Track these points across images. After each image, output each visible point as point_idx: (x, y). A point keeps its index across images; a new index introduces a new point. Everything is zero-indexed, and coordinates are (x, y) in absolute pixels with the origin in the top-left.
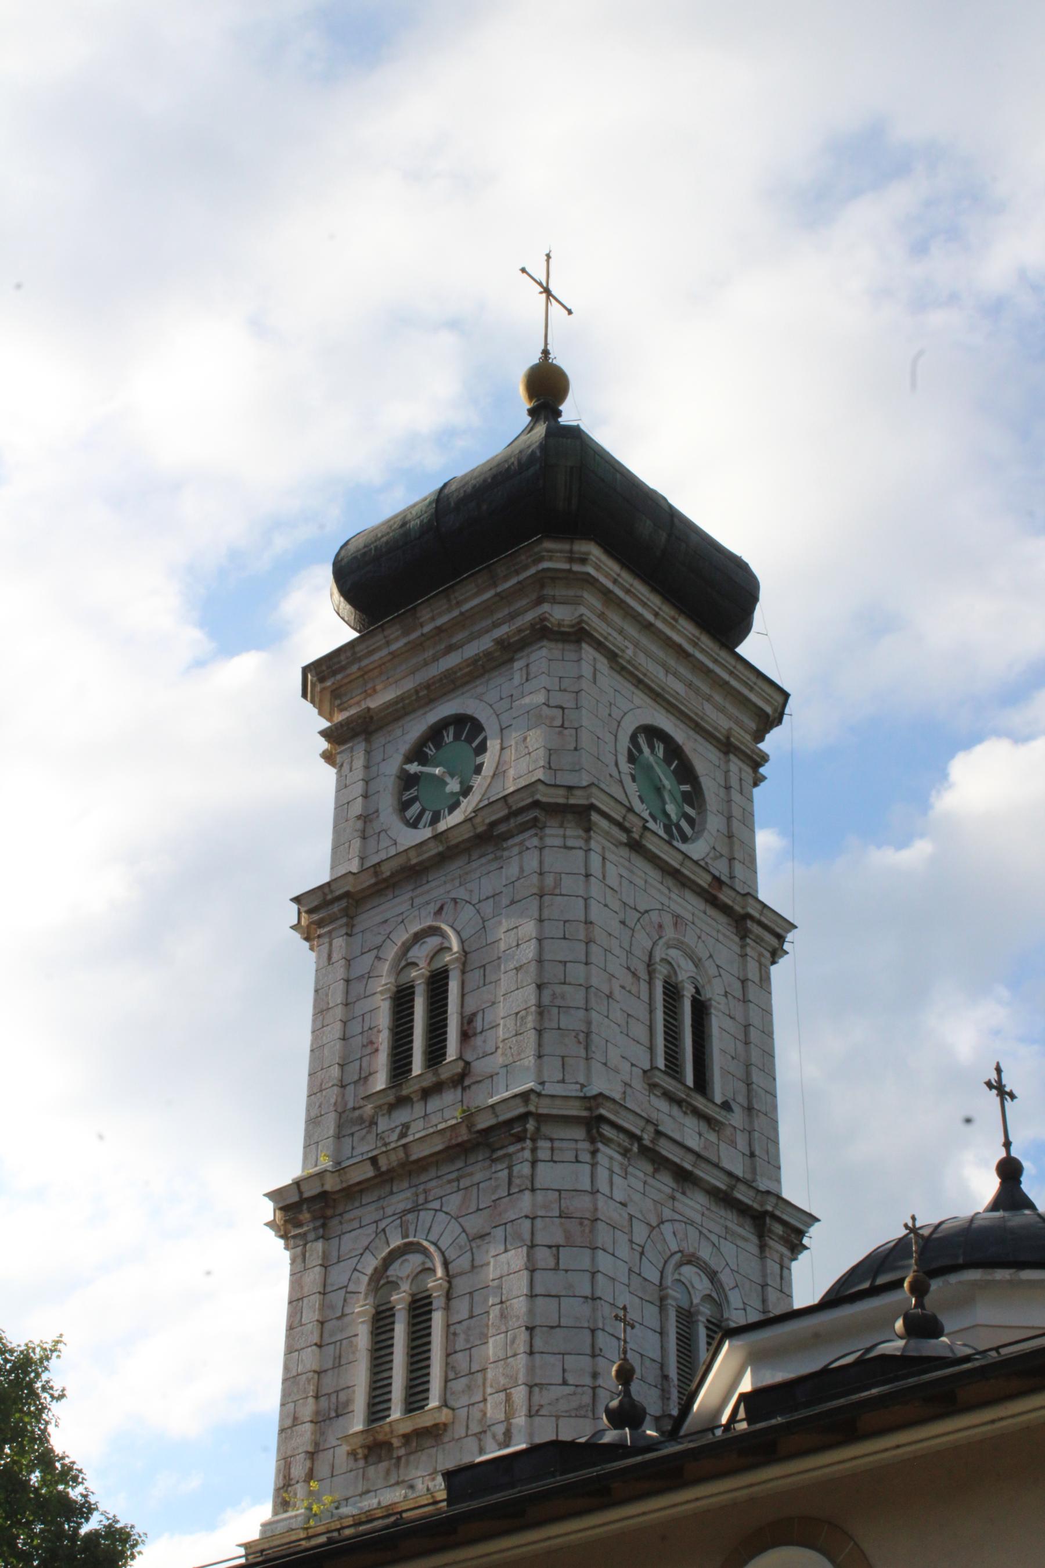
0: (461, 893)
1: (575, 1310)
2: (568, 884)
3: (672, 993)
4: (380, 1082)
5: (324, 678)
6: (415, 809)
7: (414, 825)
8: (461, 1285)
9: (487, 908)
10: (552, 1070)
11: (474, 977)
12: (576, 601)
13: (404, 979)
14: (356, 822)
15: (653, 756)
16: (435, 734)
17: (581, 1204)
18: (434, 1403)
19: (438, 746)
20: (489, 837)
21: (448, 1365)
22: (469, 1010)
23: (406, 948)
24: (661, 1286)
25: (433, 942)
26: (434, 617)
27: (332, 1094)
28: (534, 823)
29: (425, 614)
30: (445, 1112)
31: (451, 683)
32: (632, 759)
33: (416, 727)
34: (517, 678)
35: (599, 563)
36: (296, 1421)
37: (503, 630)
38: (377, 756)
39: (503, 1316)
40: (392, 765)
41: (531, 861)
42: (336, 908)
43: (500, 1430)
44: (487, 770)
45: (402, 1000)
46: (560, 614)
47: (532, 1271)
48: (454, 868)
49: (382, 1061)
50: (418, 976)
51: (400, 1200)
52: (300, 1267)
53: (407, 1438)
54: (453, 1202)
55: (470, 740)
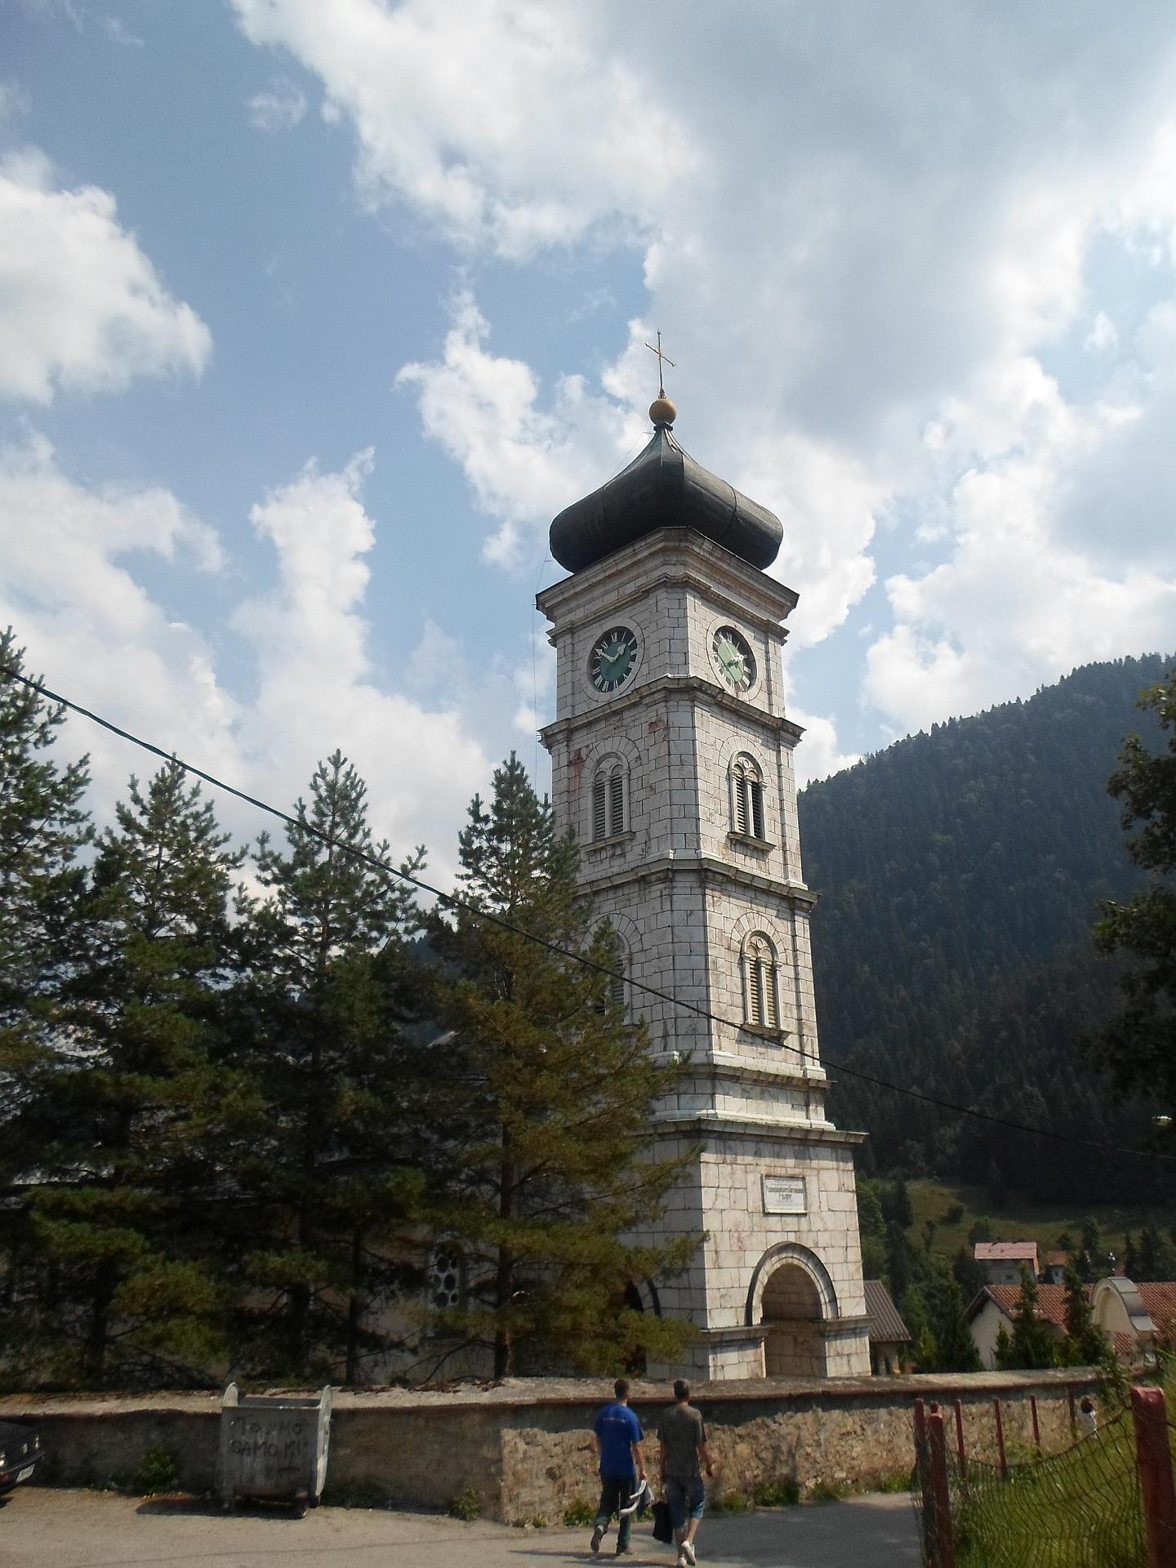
3: (742, 785)
11: (635, 785)
15: (726, 643)
16: (607, 637)
19: (609, 642)
23: (599, 762)
24: (741, 952)
25: (613, 761)
31: (617, 609)
32: (715, 649)
33: (597, 632)
40: (586, 655)
50: (606, 780)
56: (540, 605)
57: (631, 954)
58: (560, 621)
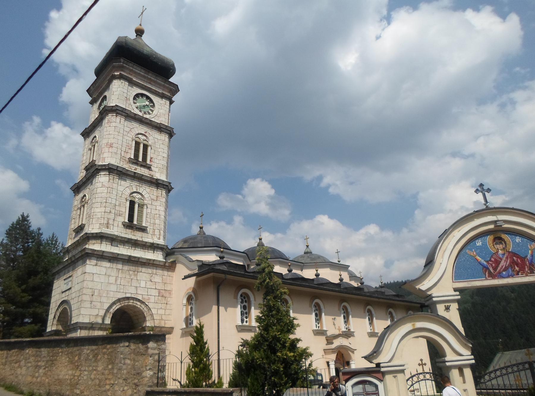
0: (150, 133)
13: (137, 139)
16: (142, 95)
26: (150, 76)
29: (150, 74)
36: (110, 212)
42: (124, 114)
43: (158, 236)
45: (137, 144)
49: (133, 152)
52: (111, 181)
53: (137, 228)
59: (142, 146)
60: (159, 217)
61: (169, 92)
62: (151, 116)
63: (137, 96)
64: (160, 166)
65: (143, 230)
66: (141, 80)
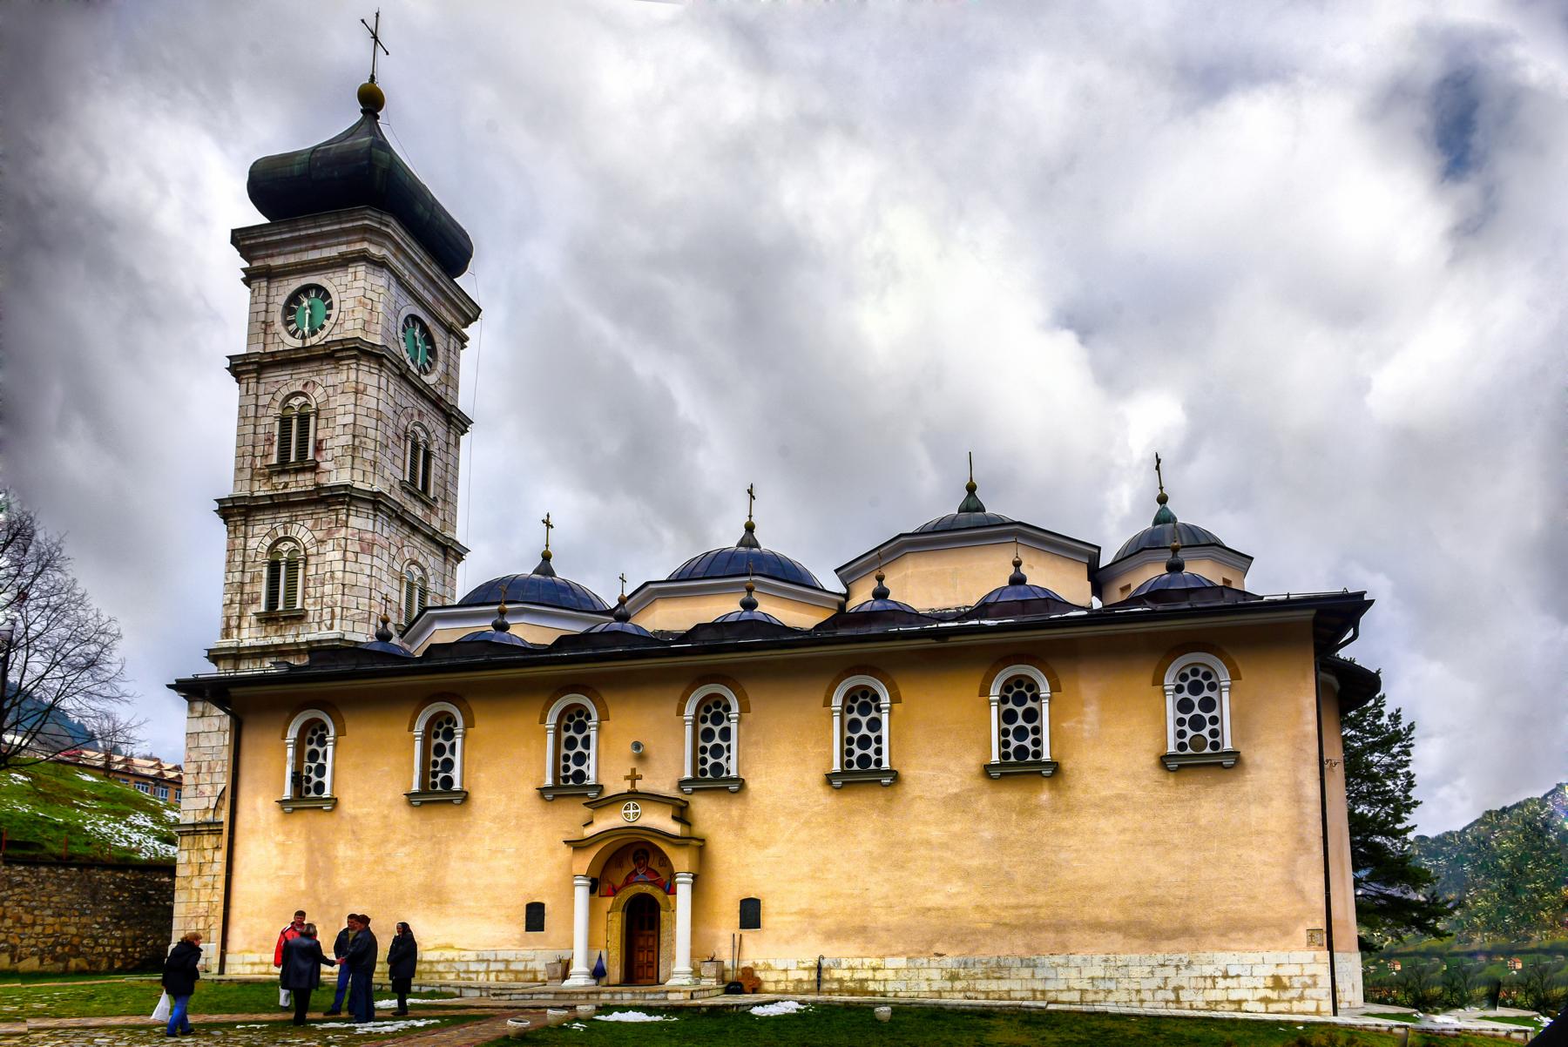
0: (316, 379)
1: (363, 580)
2: (370, 390)
4: (274, 460)
5: (241, 238)
6: (293, 327)
7: (293, 335)
8: (312, 560)
9: (330, 391)
10: (358, 476)
11: (322, 423)
12: (382, 245)
14: (260, 325)
16: (305, 290)
17: (369, 536)
18: (298, 606)
20: (332, 355)
21: (304, 592)
22: (320, 436)
23: (288, 398)
25: (302, 399)
27: (249, 459)
28: (355, 357)
30: (305, 482)
34: (350, 277)
35: (394, 229)
37: (343, 249)
38: (273, 292)
39: (332, 578)
40: (281, 300)
41: (353, 376)
44: (333, 320)
45: (285, 422)
46: (374, 250)
47: (345, 560)
48: (315, 366)
51: (284, 516)
53: (285, 618)
54: (309, 523)
55: (324, 300)
56: (234, 241)
57: (306, 556)
58: (256, 264)
59: (295, 422)
60: (332, 578)
61: (363, 240)
62: (325, 332)
63: (294, 298)
64: (338, 452)
65: (300, 617)
66: (295, 252)
